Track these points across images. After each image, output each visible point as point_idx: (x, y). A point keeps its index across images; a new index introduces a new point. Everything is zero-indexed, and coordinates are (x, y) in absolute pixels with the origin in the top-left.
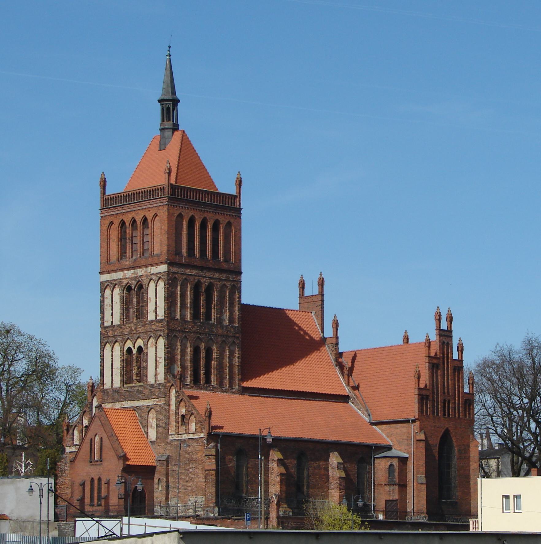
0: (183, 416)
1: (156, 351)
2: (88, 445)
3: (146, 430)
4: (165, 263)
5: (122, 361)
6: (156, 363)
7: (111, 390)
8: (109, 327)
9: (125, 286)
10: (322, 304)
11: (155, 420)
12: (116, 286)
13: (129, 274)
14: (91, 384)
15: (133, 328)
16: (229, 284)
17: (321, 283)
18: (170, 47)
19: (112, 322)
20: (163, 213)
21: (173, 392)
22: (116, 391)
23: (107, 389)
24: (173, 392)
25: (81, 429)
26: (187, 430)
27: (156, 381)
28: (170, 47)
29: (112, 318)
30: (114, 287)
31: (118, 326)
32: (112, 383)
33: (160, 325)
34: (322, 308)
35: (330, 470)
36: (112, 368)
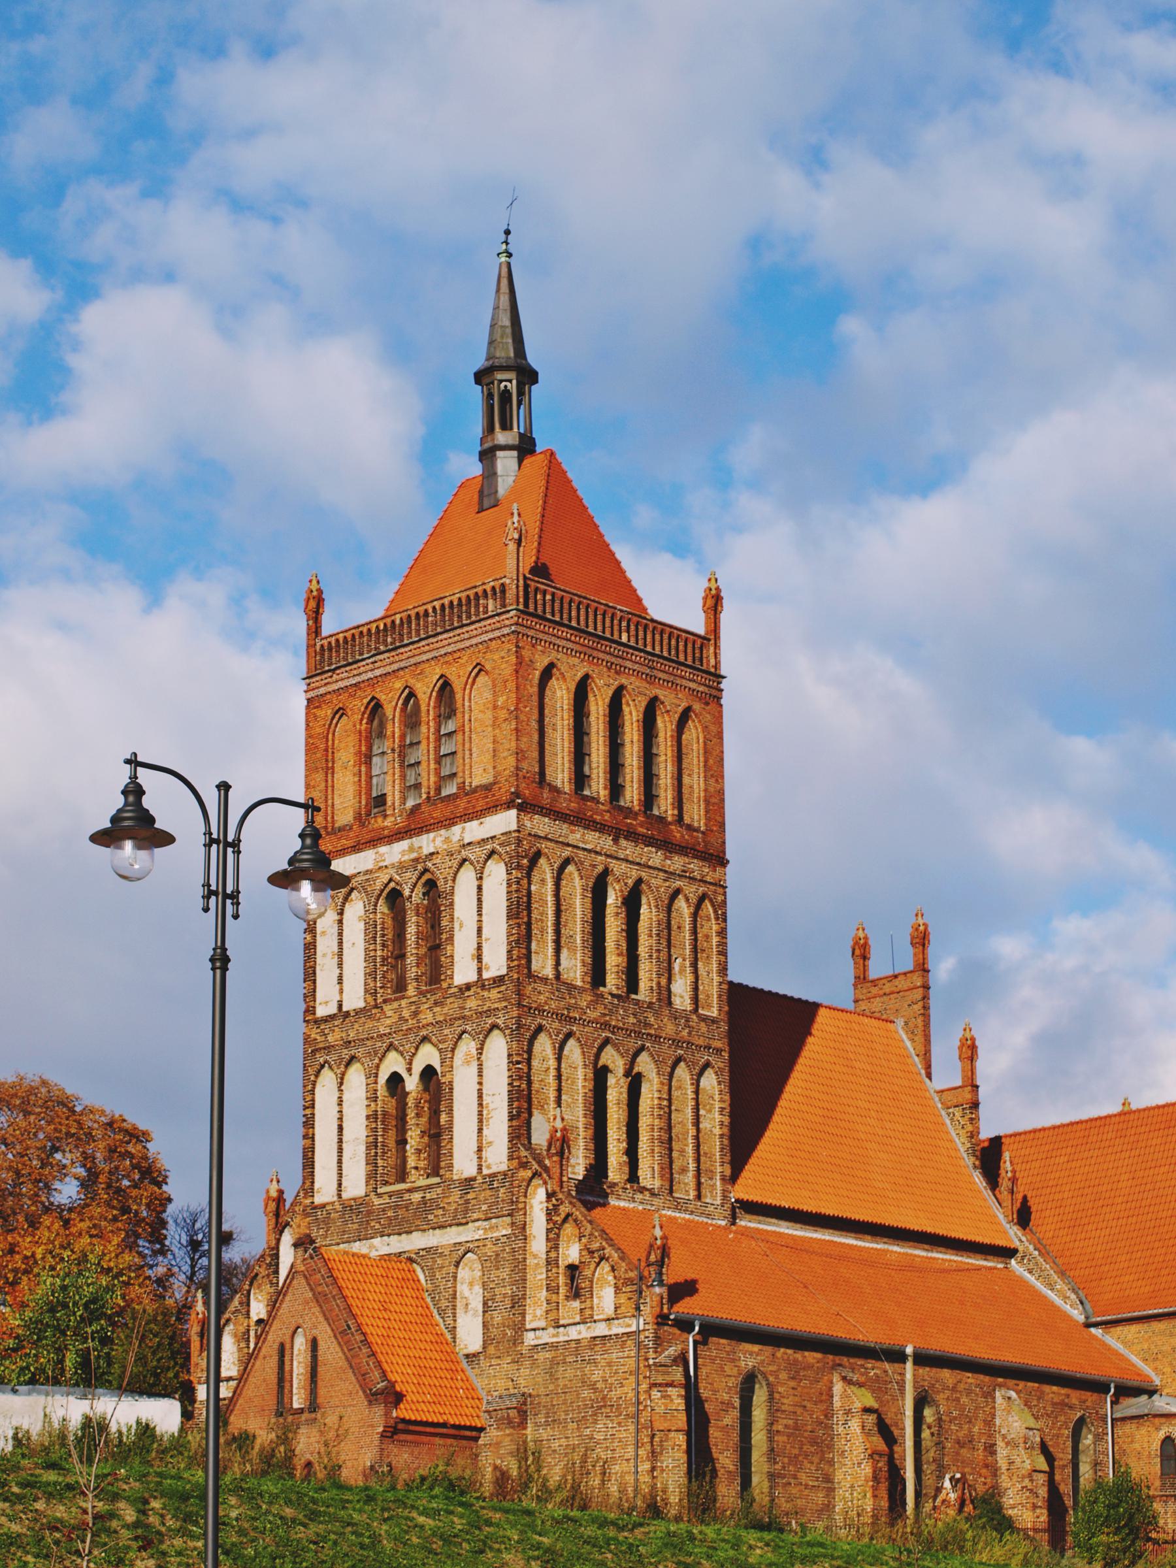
0: (572, 1269)
1: (480, 1075)
2: (273, 1362)
3: (449, 1321)
4: (509, 805)
5: (372, 1117)
6: (480, 1113)
7: (338, 1207)
8: (332, 1017)
9: (382, 891)
10: (925, 997)
11: (478, 1289)
13: (395, 852)
14: (274, 1194)
15: (406, 1014)
16: (692, 891)
17: (921, 940)
18: (507, 232)
19: (340, 1006)
20: (501, 660)
22: (352, 1208)
23: (323, 1206)
25: (242, 1329)
26: (588, 1312)
27: (480, 1168)
28: (507, 232)
29: (341, 991)
31: (358, 1012)
32: (340, 1185)
33: (494, 994)
34: (926, 1008)
35: (1002, 1452)
36: (340, 1141)
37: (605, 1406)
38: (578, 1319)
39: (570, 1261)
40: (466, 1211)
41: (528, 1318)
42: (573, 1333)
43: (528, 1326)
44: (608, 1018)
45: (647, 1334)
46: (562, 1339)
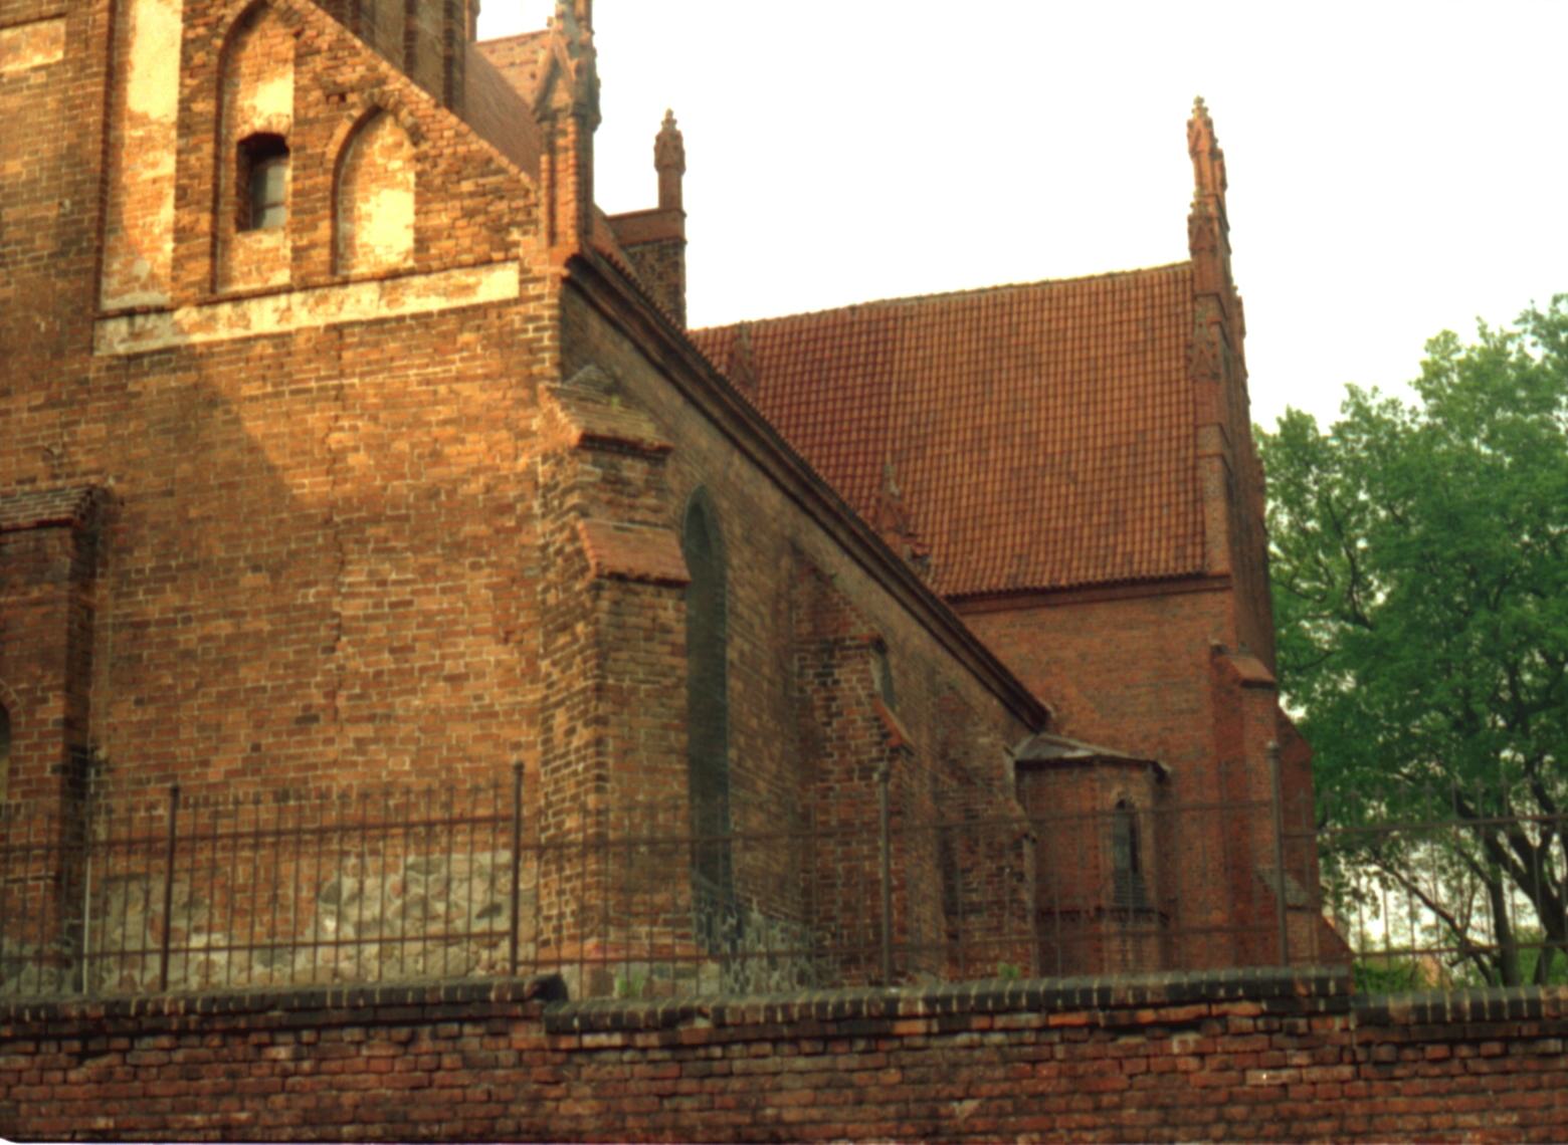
0: (265, 148)
37: (376, 520)
38: (282, 277)
39: (258, 124)
41: (111, 284)
42: (264, 318)
43: (110, 304)
45: (531, 308)
46: (223, 333)
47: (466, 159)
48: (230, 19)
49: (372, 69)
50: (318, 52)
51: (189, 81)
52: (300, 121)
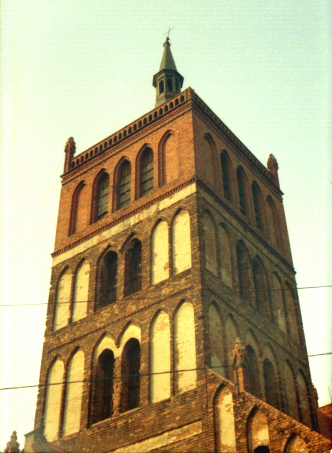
4: (189, 182)
9: (102, 253)
12: (86, 261)
15: (116, 312)
19: (70, 320)
21: (227, 400)
24: (227, 400)
30: (79, 265)
39: (259, 443)
40: (161, 425)
44: (250, 317)
47: (323, 445)
48: (247, 414)
49: (291, 422)
50: (274, 420)
51: (238, 434)
52: (272, 441)
